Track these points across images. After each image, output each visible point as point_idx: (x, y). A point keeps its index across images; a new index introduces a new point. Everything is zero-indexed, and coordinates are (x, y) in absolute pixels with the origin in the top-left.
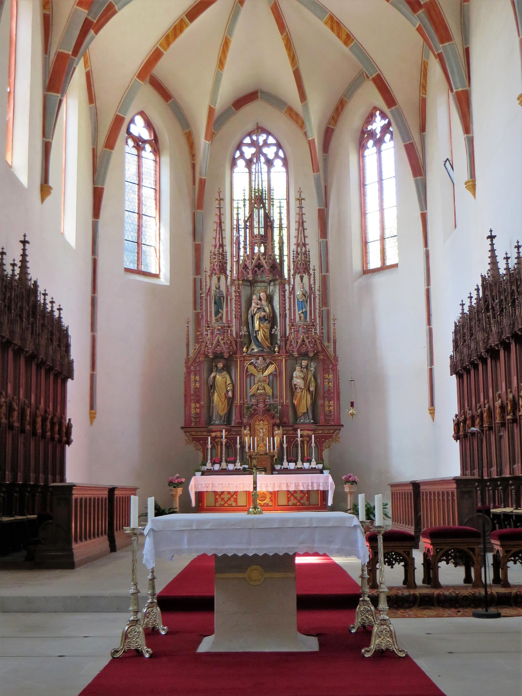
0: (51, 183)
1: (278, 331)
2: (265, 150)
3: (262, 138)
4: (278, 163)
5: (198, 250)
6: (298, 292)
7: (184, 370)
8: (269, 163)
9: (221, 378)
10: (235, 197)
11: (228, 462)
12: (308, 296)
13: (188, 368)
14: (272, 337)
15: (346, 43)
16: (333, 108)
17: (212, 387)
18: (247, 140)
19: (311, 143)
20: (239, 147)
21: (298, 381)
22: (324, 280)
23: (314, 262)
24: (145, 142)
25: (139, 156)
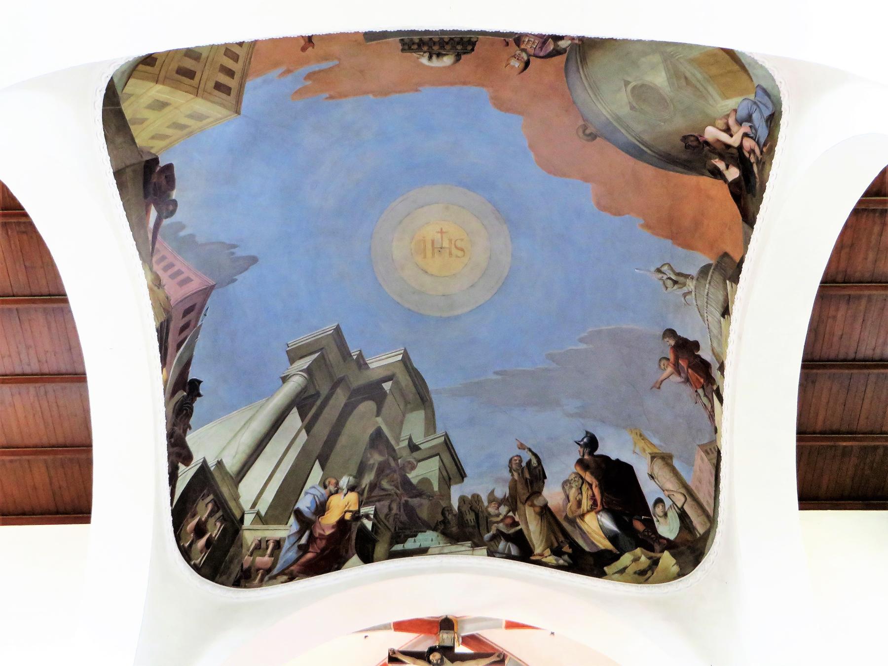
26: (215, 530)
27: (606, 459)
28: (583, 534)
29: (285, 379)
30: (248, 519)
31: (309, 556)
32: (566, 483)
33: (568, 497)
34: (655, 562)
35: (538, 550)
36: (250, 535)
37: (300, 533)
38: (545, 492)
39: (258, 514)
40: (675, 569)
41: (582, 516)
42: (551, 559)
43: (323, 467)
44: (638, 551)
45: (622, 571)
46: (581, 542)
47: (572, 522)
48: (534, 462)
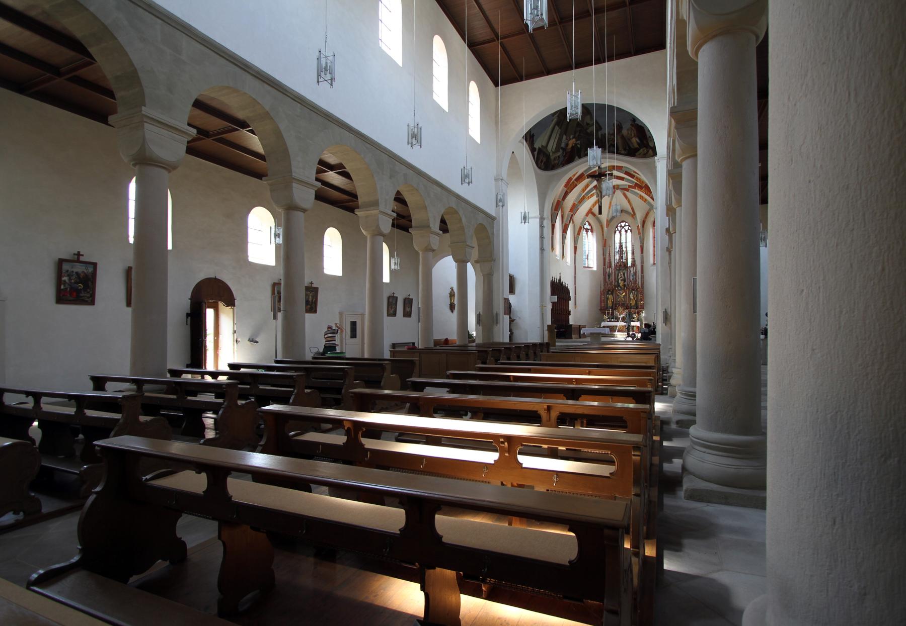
0: (564, 255)
1: (626, 283)
2: (625, 227)
3: (624, 223)
4: (629, 231)
5: (604, 259)
6: (632, 272)
7: (600, 294)
8: (626, 231)
9: (610, 296)
10: (616, 242)
11: (612, 319)
12: (635, 273)
13: (601, 294)
14: (624, 285)
15: (645, 202)
16: (645, 215)
17: (608, 299)
18: (619, 225)
19: (638, 227)
20: (617, 227)
21: (632, 298)
22: (642, 267)
23: (638, 263)
24: (589, 229)
25: (587, 234)
26: (545, 160)
27: (638, 124)
28: (632, 143)
29: (552, 121)
30: (551, 154)
31: (566, 158)
32: (628, 130)
33: (628, 133)
34: (648, 152)
35: (620, 149)
36: (552, 158)
37: (563, 153)
38: (623, 131)
39: (553, 152)
40: (652, 154)
41: (632, 138)
42: (623, 152)
43: (565, 135)
44: (645, 148)
45: (640, 154)
46: (631, 146)
47: (629, 140)
48: (620, 124)
